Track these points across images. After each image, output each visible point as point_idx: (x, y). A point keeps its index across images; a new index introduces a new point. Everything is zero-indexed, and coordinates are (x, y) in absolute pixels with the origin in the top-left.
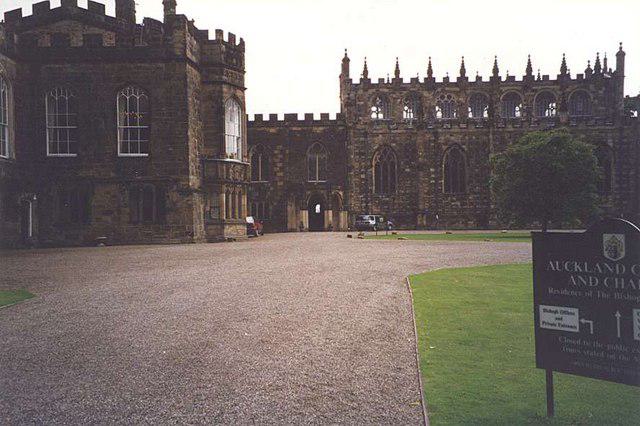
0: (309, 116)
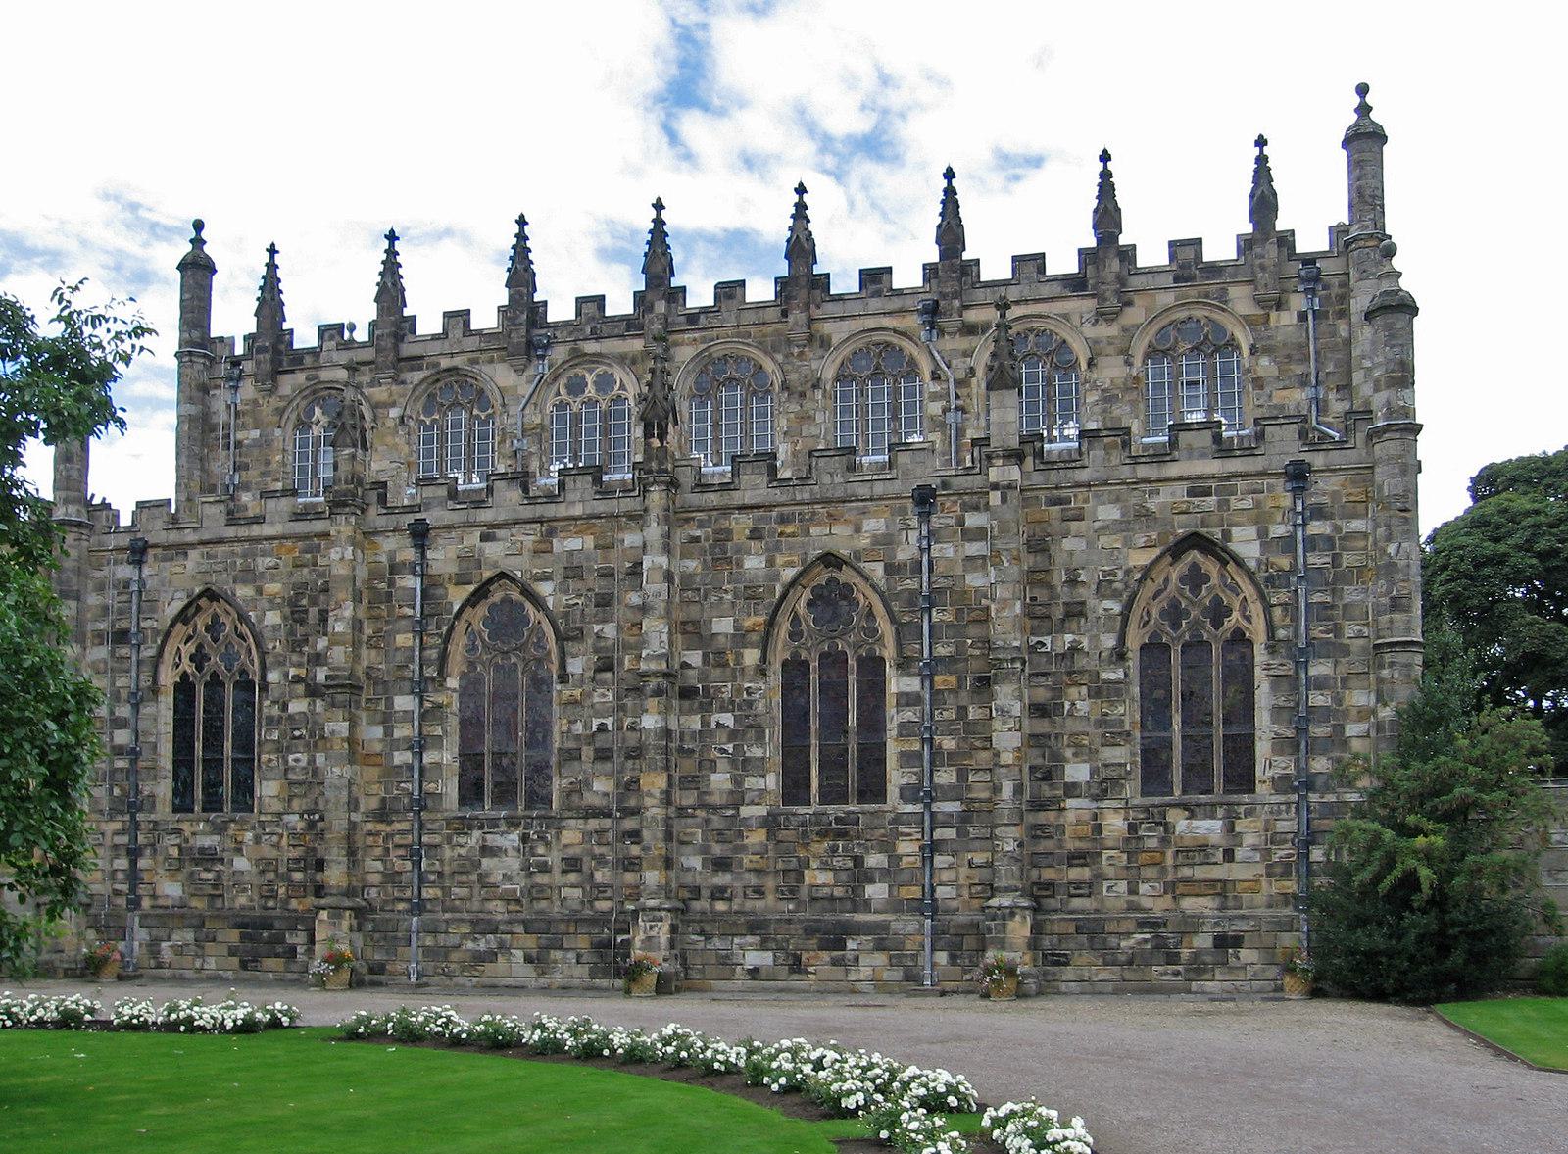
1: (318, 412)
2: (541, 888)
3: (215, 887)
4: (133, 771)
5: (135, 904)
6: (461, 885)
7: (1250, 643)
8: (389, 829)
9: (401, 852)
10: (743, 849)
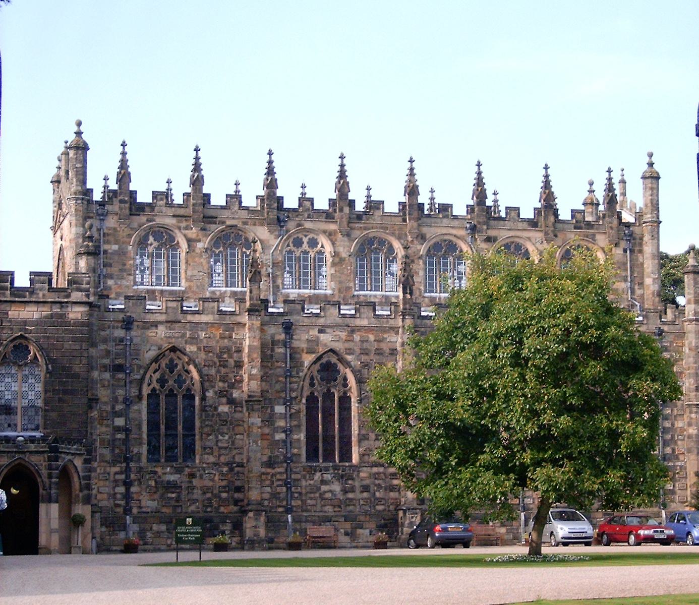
1: (151, 239)
2: (351, 500)
3: (177, 501)
4: (126, 441)
5: (127, 511)
6: (311, 499)
8: (273, 471)
9: (280, 483)
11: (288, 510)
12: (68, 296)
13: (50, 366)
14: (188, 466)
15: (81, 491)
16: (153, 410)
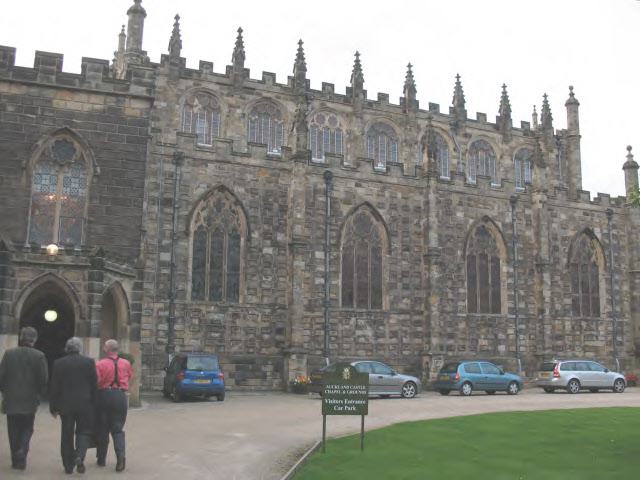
0: (48, 62)
2: (382, 345)
3: (220, 341)
4: (170, 278)
6: (347, 343)
7: (597, 267)
9: (318, 326)
10: (457, 330)
11: (326, 353)
12: (127, 89)
13: (98, 170)
14: (232, 306)
15: (129, 323)
16: (199, 249)
